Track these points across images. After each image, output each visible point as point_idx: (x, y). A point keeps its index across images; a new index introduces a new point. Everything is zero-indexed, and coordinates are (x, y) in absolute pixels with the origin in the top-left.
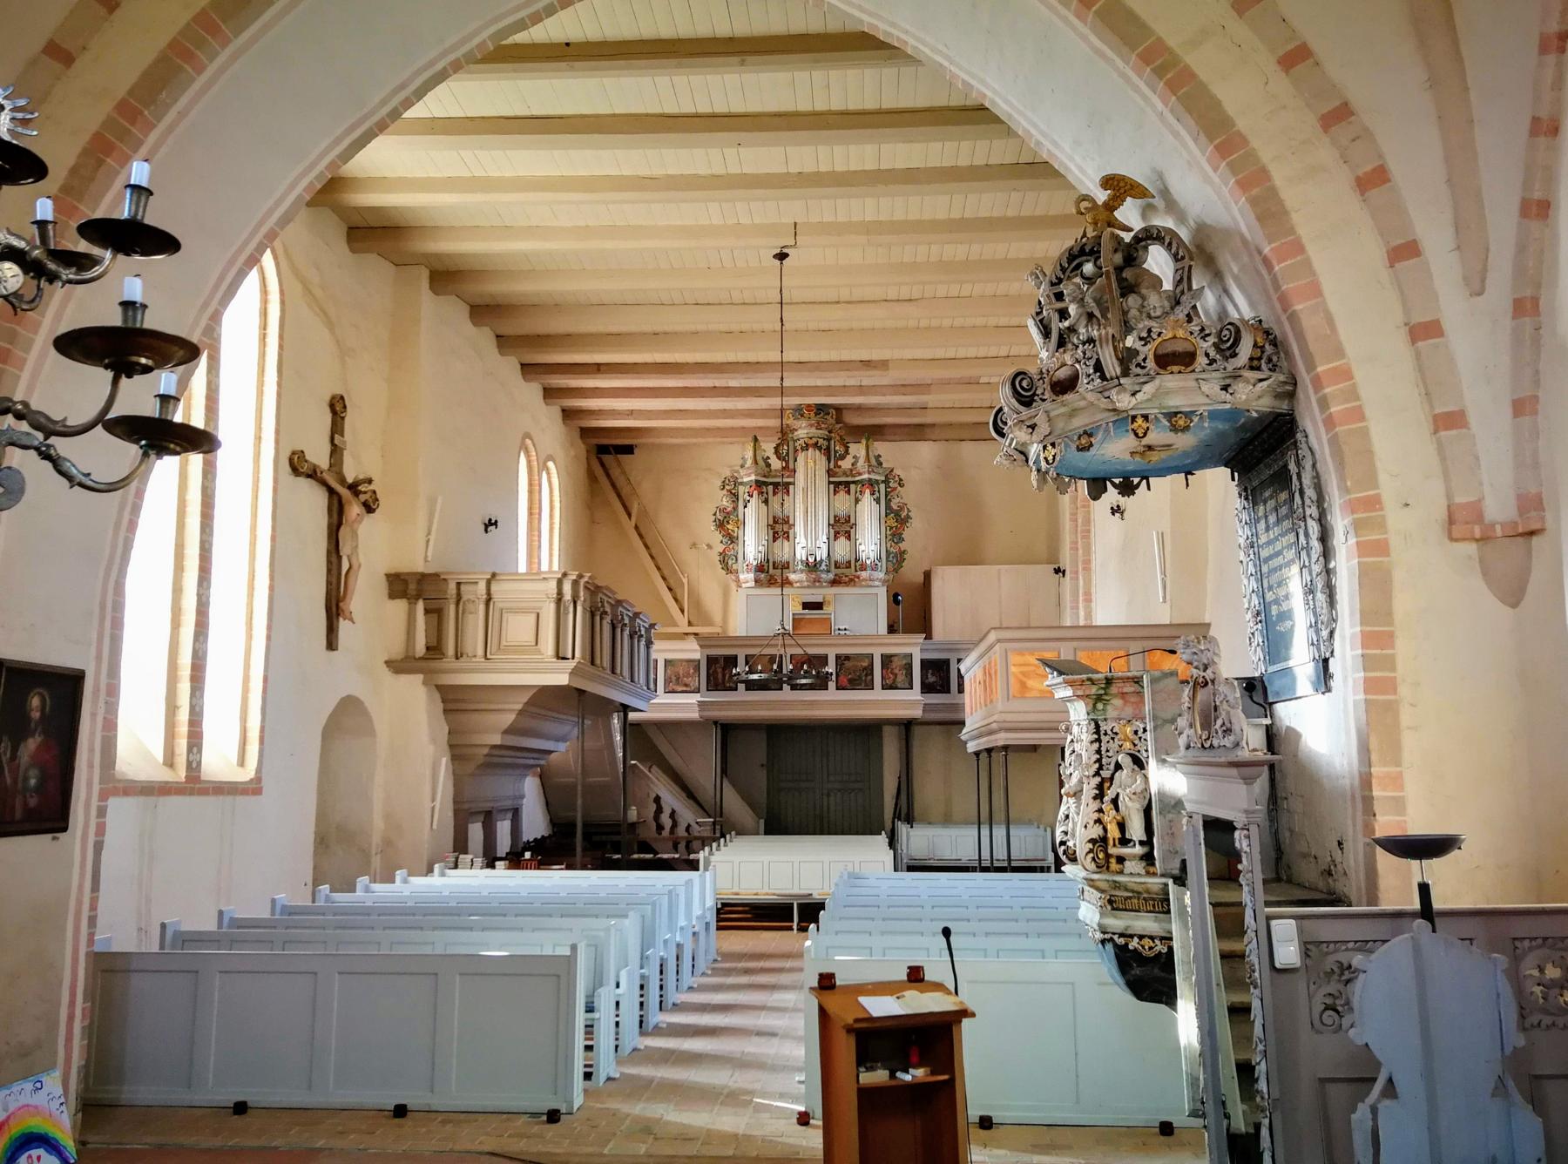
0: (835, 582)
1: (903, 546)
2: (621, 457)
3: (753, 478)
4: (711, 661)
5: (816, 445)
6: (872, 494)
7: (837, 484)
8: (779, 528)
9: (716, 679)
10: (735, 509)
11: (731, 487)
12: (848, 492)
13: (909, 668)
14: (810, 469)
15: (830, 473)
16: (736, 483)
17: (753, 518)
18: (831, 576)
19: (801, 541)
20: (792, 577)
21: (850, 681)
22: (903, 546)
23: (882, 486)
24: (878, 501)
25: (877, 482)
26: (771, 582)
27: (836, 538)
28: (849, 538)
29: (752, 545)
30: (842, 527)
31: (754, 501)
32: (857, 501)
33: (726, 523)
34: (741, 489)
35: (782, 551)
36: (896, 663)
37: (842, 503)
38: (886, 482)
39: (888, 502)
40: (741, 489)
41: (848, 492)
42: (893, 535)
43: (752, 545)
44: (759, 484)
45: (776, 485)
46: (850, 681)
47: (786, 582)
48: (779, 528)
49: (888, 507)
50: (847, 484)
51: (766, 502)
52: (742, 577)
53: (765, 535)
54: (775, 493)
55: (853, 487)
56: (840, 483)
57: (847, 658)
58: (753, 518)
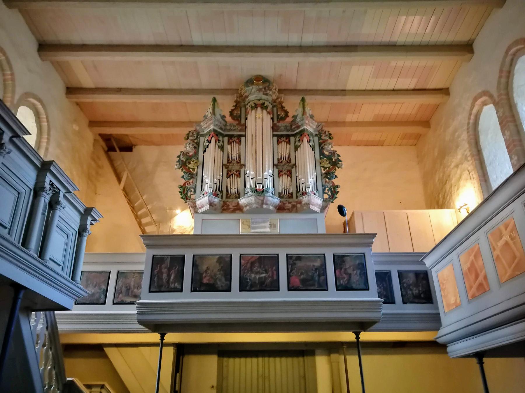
0: (280, 209)
1: (336, 181)
2: (123, 153)
3: (212, 127)
4: (156, 261)
5: (263, 106)
6: (309, 142)
7: (279, 137)
8: (232, 168)
9: (160, 278)
10: (196, 153)
11: (195, 138)
12: (289, 143)
13: (362, 267)
14: (259, 123)
15: (274, 128)
16: (199, 135)
17: (212, 159)
18: (276, 201)
19: (250, 172)
20: (243, 201)
21: (303, 281)
22: (336, 181)
23: (316, 139)
24: (313, 149)
25: (312, 134)
26: (225, 208)
27: (279, 175)
28: (290, 175)
29: (209, 178)
30: (285, 167)
31: (212, 146)
32: (296, 148)
33: (188, 164)
34: (202, 139)
35: (234, 184)
36: (349, 264)
37: (285, 150)
38: (319, 135)
39: (321, 149)
40: (202, 139)
41: (289, 143)
42: (327, 174)
43: (209, 178)
44: (216, 134)
45: (230, 137)
46: (303, 281)
47: (238, 209)
48: (232, 168)
49: (322, 153)
50: (288, 136)
51: (222, 148)
52: (199, 203)
53: (220, 173)
54: (229, 143)
55: (292, 139)
56: (282, 136)
57: (299, 258)
58: (212, 159)
